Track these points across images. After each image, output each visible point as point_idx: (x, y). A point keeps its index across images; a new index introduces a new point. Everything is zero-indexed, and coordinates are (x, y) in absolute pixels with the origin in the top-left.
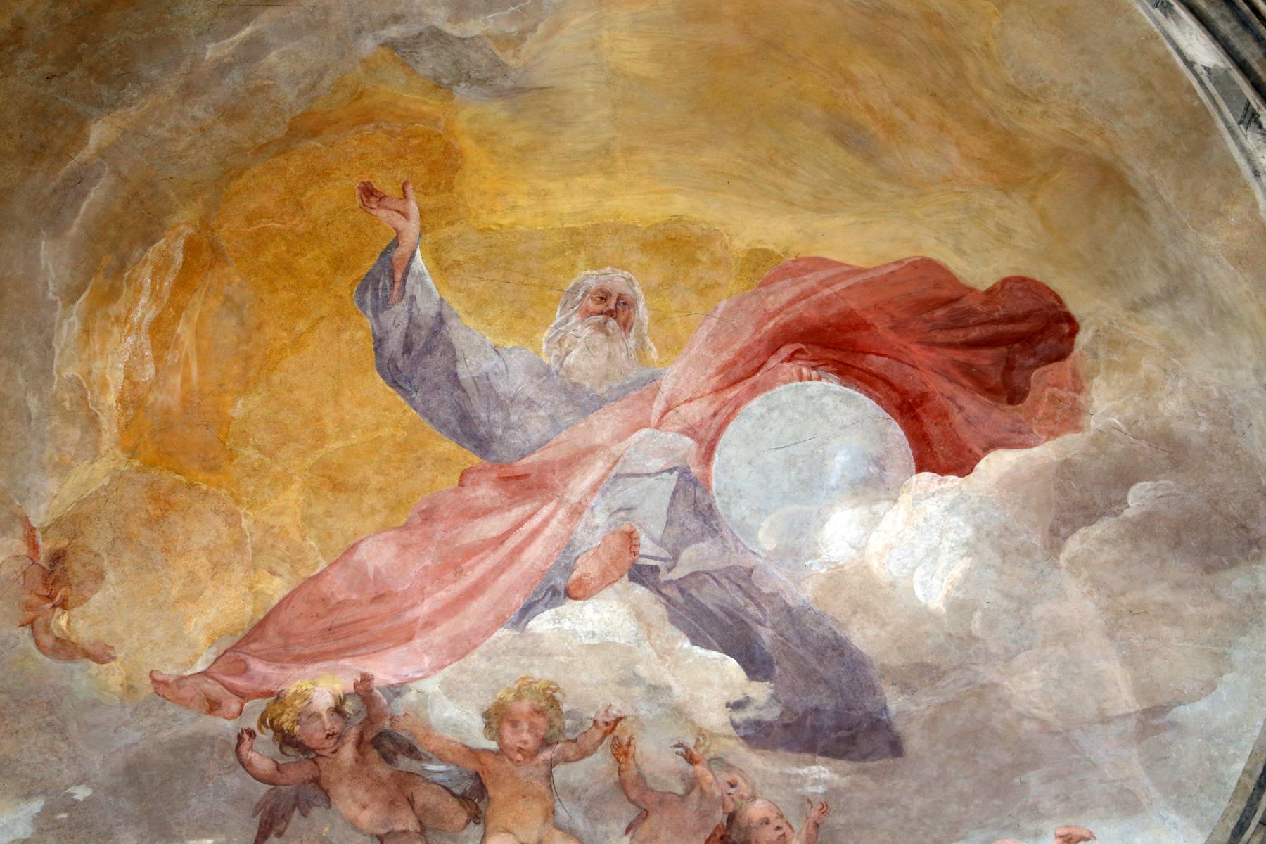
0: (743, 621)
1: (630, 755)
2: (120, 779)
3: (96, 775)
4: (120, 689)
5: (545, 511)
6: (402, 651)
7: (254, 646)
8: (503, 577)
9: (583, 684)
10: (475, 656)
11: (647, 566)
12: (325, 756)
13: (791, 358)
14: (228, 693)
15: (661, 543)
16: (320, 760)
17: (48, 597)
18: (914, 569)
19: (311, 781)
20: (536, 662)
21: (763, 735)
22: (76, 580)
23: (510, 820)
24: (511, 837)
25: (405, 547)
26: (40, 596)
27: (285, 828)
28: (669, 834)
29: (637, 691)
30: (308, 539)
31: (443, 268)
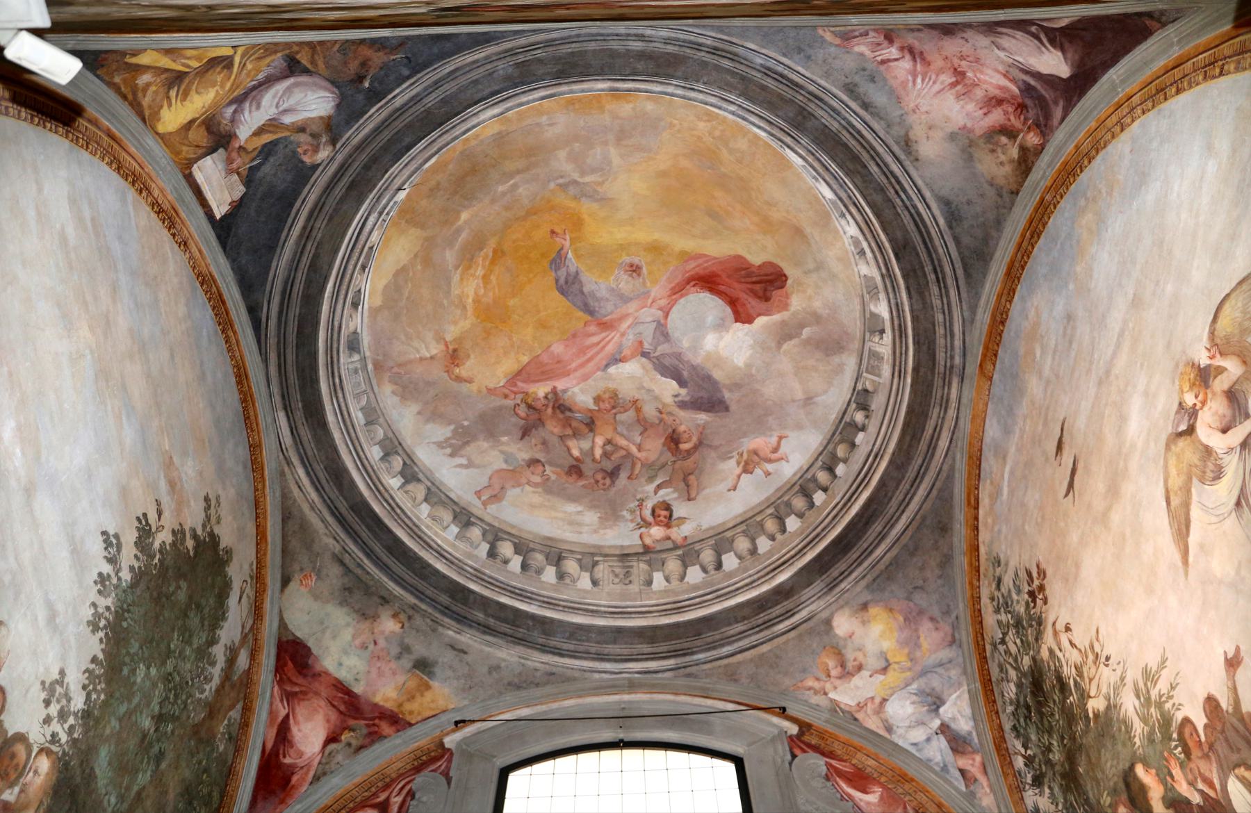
5: (613, 334)
6: (566, 379)
10: (590, 380)
13: (694, 286)
25: (567, 346)
29: (643, 391)
31: (578, 257)
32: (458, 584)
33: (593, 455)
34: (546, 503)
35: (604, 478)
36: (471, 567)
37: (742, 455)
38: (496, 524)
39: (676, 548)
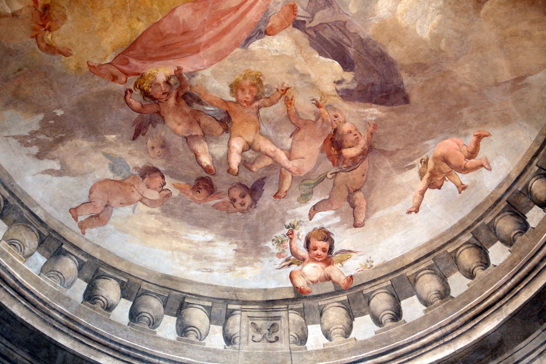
0: (342, 45)
1: (293, 104)
2: (76, 107)
3: (65, 105)
4: (74, 68)
6: (195, 57)
7: (131, 53)
8: (238, 25)
9: (273, 73)
10: (226, 60)
11: (300, 20)
12: (163, 102)
14: (121, 73)
15: (307, 10)
16: (160, 104)
17: (42, 25)
18: (416, 21)
19: (156, 113)
20: (252, 63)
21: (349, 95)
22: (54, 19)
23: (241, 131)
24: (242, 139)
25: (196, 10)
26: (39, 25)
27: (146, 132)
28: (309, 137)
29: (295, 76)
30: (154, 5)
32: (42, 335)
33: (229, 164)
34: (165, 229)
35: (243, 197)
36: (61, 314)
37: (426, 163)
38: (98, 255)
39: (338, 291)
